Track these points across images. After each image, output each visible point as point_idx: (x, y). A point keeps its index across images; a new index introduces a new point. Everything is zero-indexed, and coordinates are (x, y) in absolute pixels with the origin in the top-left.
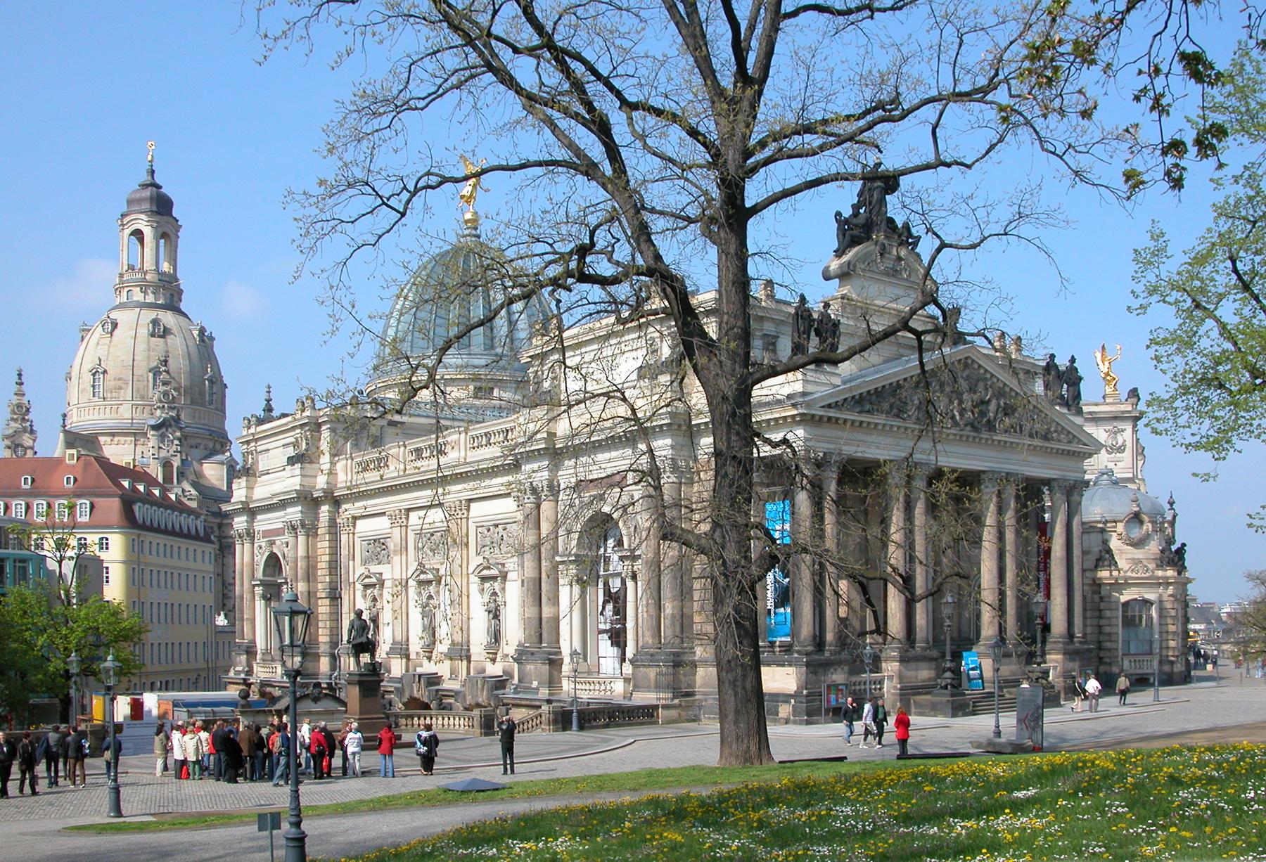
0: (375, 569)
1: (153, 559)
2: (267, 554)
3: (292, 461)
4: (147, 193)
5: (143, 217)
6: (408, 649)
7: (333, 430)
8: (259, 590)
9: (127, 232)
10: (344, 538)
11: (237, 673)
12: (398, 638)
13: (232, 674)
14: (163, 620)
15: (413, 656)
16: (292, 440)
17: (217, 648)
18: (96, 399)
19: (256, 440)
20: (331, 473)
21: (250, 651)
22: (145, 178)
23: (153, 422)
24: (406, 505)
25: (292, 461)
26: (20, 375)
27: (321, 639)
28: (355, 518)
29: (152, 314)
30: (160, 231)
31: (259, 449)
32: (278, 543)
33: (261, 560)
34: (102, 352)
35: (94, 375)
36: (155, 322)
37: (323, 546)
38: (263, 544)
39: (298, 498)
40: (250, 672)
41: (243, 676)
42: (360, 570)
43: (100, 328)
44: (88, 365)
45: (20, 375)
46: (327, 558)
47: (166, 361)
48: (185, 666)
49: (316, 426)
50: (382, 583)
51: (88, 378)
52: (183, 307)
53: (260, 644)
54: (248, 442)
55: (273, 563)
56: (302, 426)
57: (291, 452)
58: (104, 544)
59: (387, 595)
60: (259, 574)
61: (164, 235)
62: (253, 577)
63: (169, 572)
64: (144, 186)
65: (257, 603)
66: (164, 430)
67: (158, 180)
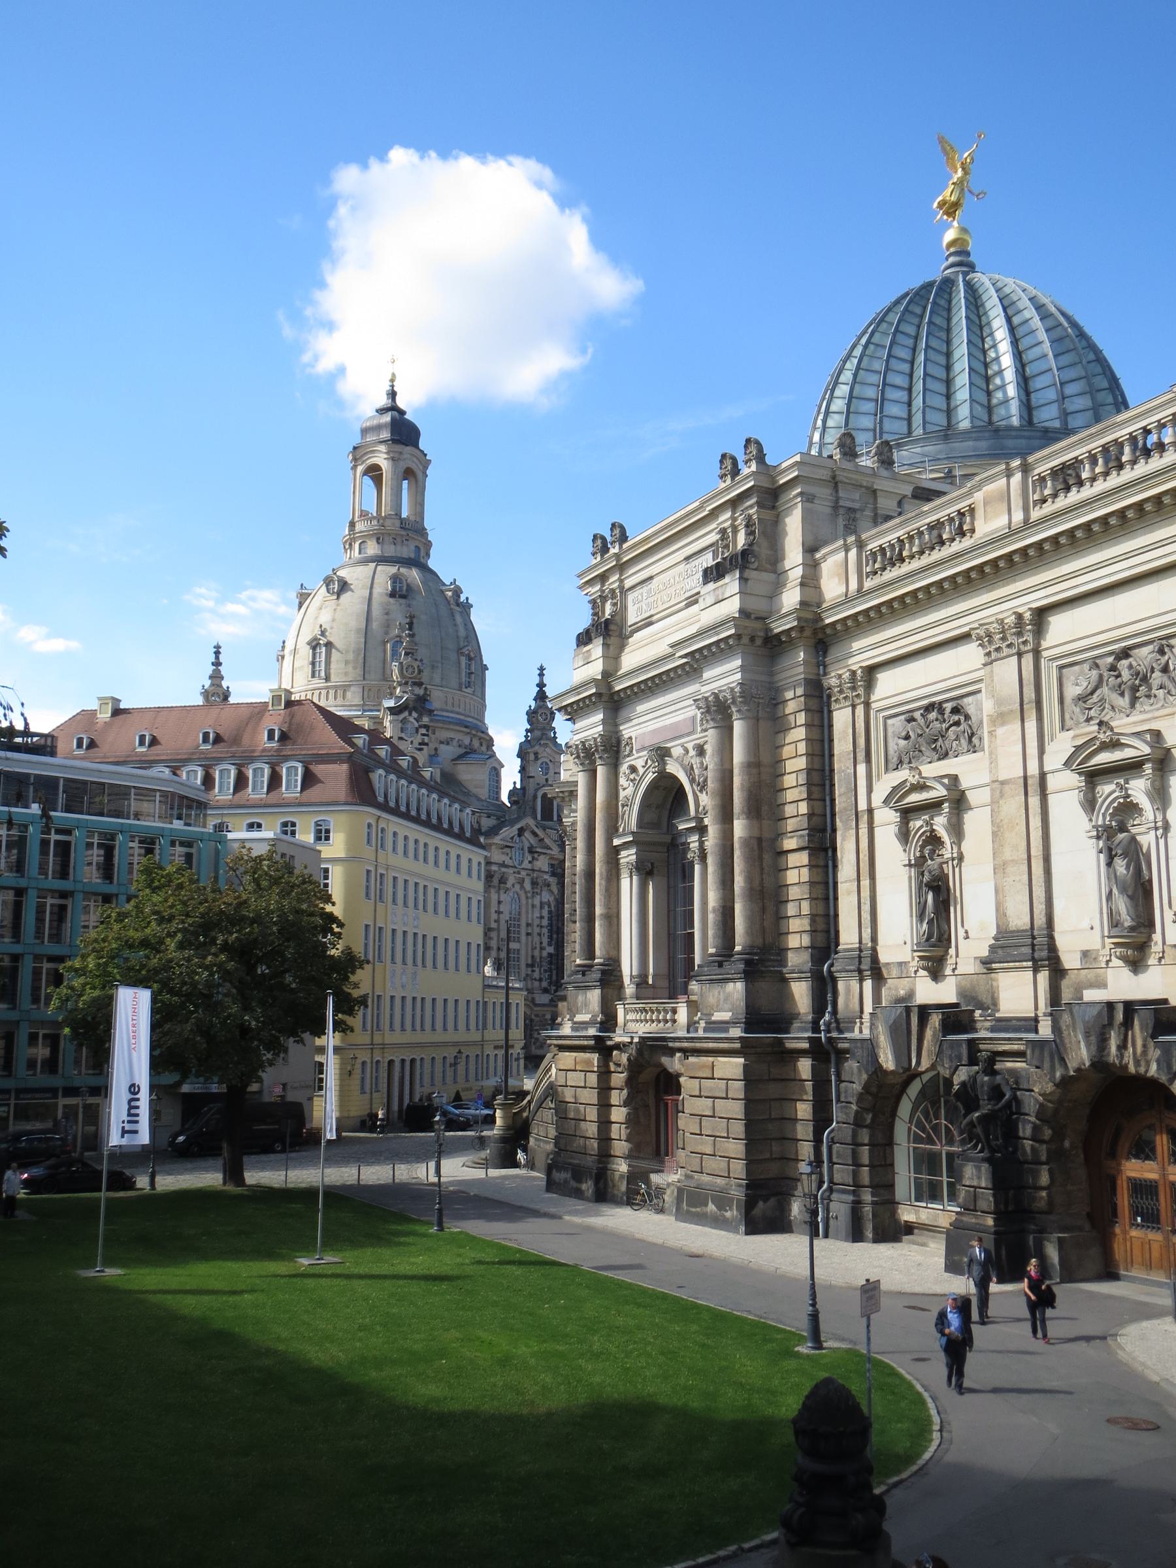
0: (932, 769)
1: (397, 860)
2: (650, 777)
3: (714, 574)
4: (387, 418)
5: (383, 448)
6: (1052, 948)
7: (807, 498)
8: (628, 857)
9: (360, 469)
10: (841, 718)
11: (577, 1026)
12: (1019, 919)
13: (567, 1030)
14: (410, 960)
15: (1070, 960)
16: (714, 537)
17: (485, 1010)
18: (316, 680)
19: (621, 567)
20: (810, 581)
21: (610, 978)
22: (383, 401)
23: (391, 703)
24: (1040, 599)
25: (714, 574)
26: (217, 653)
27: (793, 941)
28: (871, 671)
29: (393, 570)
30: (403, 465)
31: (628, 583)
32: (677, 752)
33: (632, 792)
34: (325, 618)
35: (314, 648)
36: (395, 579)
37: (796, 740)
38: (639, 764)
39: (738, 636)
40: (608, 1022)
41: (592, 1032)
42: (885, 785)
43: (324, 588)
44: (306, 636)
45: (217, 653)
46: (802, 763)
47: (411, 625)
48: (439, 1037)
49: (770, 496)
50: (959, 802)
51: (305, 652)
52: (432, 564)
53: (628, 966)
54: (603, 578)
55: (667, 797)
56: (734, 503)
57: (708, 560)
58: (323, 835)
59: (976, 822)
60: (631, 819)
61: (408, 474)
62: (612, 830)
63: (422, 883)
64: (382, 411)
65: (625, 883)
66: (406, 714)
67: (401, 403)
